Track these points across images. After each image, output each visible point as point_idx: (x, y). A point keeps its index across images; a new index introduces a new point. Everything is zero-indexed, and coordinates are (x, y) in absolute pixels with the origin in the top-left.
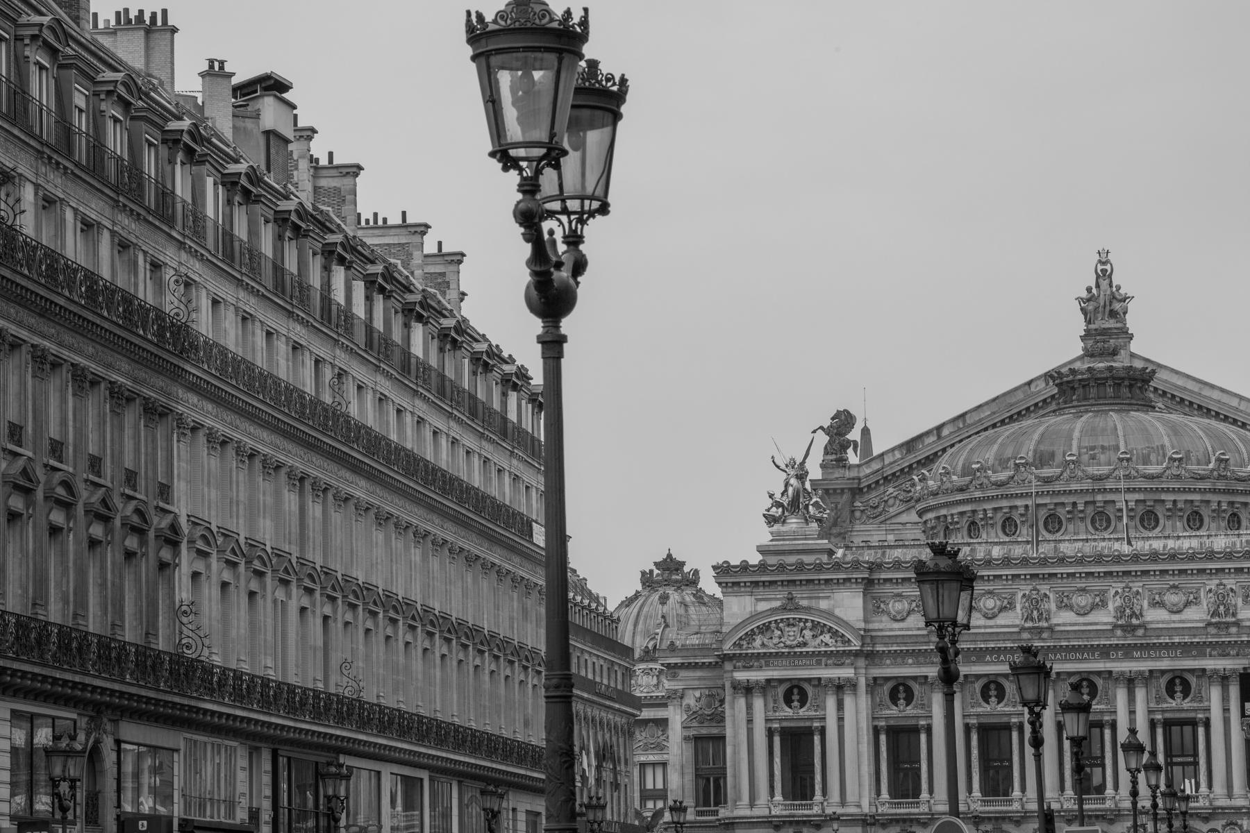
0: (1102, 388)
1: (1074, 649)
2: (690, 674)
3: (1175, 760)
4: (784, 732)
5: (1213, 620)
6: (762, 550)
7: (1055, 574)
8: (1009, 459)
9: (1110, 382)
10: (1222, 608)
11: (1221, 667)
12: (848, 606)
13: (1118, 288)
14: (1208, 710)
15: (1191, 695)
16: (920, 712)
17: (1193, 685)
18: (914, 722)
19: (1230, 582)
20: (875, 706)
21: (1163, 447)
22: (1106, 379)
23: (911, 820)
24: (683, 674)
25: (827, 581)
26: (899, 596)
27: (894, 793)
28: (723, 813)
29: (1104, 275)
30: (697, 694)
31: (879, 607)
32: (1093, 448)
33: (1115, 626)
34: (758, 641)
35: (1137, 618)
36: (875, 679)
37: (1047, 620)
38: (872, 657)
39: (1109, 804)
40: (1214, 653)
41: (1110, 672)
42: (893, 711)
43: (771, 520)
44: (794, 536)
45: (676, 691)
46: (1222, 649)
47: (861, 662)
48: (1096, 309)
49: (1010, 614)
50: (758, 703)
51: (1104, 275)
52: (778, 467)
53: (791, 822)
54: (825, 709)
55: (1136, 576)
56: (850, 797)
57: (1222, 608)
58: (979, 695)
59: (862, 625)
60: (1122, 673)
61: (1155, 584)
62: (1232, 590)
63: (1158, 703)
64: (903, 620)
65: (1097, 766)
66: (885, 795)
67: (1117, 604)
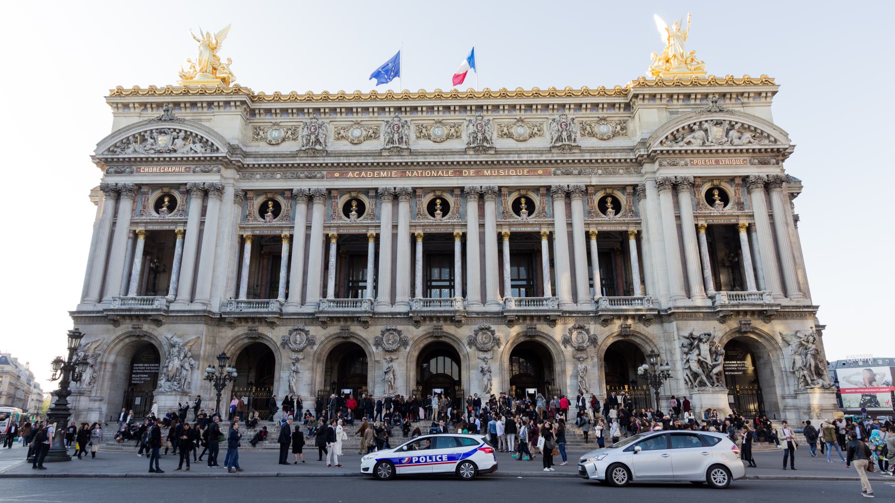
5: (557, 145)
14: (553, 224)
18: (278, 232)
19: (571, 114)
20: (246, 217)
25: (210, 104)
27: (249, 295)
31: (258, 134)
34: (132, 146)
36: (246, 192)
38: (241, 168)
39: (458, 305)
40: (559, 172)
41: (462, 189)
46: (564, 167)
47: (230, 173)
53: (131, 317)
56: (198, 296)
57: (564, 133)
58: (341, 210)
59: (234, 142)
60: (473, 189)
61: (504, 118)
64: (278, 144)
65: (445, 287)
66: (243, 297)
67: (471, 131)
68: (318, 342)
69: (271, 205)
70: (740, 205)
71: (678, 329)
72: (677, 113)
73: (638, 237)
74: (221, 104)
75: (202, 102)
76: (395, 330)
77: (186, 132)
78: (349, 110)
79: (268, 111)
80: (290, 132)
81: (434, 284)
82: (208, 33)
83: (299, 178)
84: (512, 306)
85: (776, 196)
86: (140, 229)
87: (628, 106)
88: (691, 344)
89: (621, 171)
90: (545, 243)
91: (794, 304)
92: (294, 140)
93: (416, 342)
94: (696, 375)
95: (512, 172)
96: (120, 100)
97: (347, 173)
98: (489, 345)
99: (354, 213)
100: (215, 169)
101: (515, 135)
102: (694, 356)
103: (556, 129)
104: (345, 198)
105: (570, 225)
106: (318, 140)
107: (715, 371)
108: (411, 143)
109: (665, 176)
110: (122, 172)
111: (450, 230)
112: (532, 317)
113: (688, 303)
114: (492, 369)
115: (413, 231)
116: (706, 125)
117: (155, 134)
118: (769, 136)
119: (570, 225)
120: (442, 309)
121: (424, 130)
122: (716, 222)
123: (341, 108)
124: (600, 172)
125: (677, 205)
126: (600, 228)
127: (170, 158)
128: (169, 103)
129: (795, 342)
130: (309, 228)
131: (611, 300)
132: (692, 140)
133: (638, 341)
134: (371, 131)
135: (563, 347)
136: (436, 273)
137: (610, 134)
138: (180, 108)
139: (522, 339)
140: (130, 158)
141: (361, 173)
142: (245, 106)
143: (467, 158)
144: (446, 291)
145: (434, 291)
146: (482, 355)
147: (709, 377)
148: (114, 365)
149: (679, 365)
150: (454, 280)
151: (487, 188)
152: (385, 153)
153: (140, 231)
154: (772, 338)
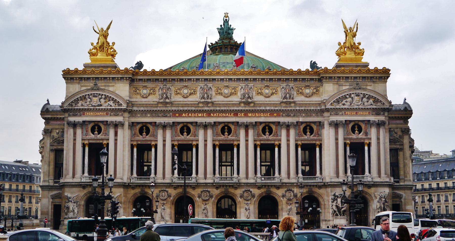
0: (226, 49)
1: (222, 111)
2: (55, 122)
3: (262, 164)
4: (90, 145)
6: (86, 66)
7: (215, 79)
8: (194, 67)
9: (229, 47)
10: (288, 95)
11: (287, 121)
12: (122, 90)
13: (231, 26)
14: (281, 140)
15: (273, 134)
16: (152, 138)
17: (274, 129)
18: (149, 143)
19: (292, 84)
20: (133, 135)
21: (248, 64)
22: (228, 45)
23: (146, 186)
24: (52, 122)
25: (113, 78)
26: (145, 87)
28: (62, 181)
29: (226, 22)
30: (58, 131)
32: (224, 63)
33: (241, 102)
35: (251, 99)
36: (133, 123)
37: (211, 99)
38: (131, 112)
39: (235, 180)
40: (284, 115)
41: (238, 122)
42: (140, 138)
43: (91, 54)
44: (101, 60)
45: (48, 130)
46: (288, 113)
47: (126, 115)
48: (223, 32)
49: (194, 96)
50: (79, 131)
51: (226, 22)
52: (95, 31)
54: (108, 135)
55: (251, 81)
57: (288, 95)
59: (128, 98)
60: (243, 123)
61: (259, 85)
62: (292, 87)
63: (258, 136)
64: (146, 97)
66: (135, 175)
68: (172, 196)
69: (144, 128)
70: (366, 134)
71: (331, 192)
72: (342, 85)
73: (320, 146)
74: (119, 78)
75: (110, 78)
76: (207, 191)
77: (105, 95)
78: (181, 80)
79: (140, 80)
80: (152, 91)
81: (223, 164)
82: (102, 29)
83: (159, 116)
84: (259, 181)
85: (382, 131)
86: (86, 142)
87: (320, 80)
88: (335, 198)
89: (314, 115)
90: (276, 149)
91: (382, 180)
92: (154, 94)
93: (217, 196)
94: (335, 211)
95: (262, 114)
96: (69, 76)
97: (182, 114)
98: (249, 198)
99: (185, 133)
100: (120, 114)
101: (264, 94)
102: (334, 204)
103: (284, 92)
104: (181, 125)
105: (288, 140)
106: (167, 96)
107: (343, 210)
108: (213, 97)
109: (332, 120)
110: (76, 115)
111: (232, 142)
112: (268, 186)
113: (337, 180)
114: (250, 208)
115: (214, 143)
116: (352, 96)
117: (91, 96)
118: (381, 101)
119: (288, 140)
120: (228, 182)
121: (219, 91)
122: (355, 141)
123: (177, 79)
124: (304, 115)
125: (337, 133)
126: (303, 142)
127: (99, 109)
128: (93, 78)
129: (378, 197)
130: (164, 141)
131: (304, 178)
132: (345, 103)
133: (316, 195)
134: (192, 91)
135: (282, 199)
136: (224, 153)
137: (311, 94)
138: (99, 80)
139: (264, 195)
140: (80, 109)
141: (189, 114)
142: (130, 79)
143: (240, 108)
144: (229, 168)
145: (223, 167)
146: (246, 202)
147: (340, 212)
148: (83, 206)
149: (331, 206)
150: (233, 162)
151: (249, 122)
152: (201, 105)
153: (86, 144)
154: (370, 195)
